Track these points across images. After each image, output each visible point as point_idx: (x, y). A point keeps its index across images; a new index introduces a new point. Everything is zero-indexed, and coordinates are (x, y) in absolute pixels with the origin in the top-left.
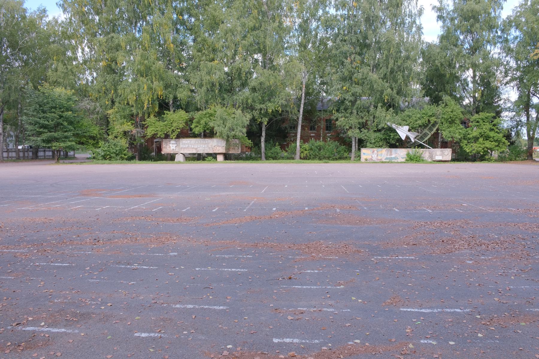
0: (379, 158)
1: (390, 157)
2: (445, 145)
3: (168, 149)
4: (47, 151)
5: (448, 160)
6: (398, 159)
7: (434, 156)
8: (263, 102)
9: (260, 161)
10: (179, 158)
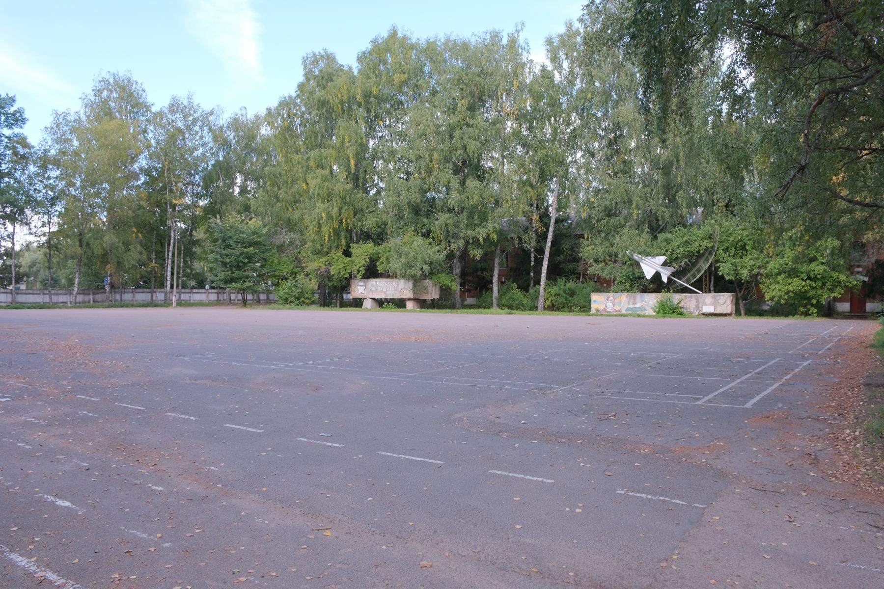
0: (617, 308)
1: (634, 306)
2: (720, 285)
3: (357, 292)
4: (184, 293)
5: (725, 312)
6: (645, 309)
7: (700, 304)
8: (471, 226)
9: (335, 308)
10: (367, 304)
